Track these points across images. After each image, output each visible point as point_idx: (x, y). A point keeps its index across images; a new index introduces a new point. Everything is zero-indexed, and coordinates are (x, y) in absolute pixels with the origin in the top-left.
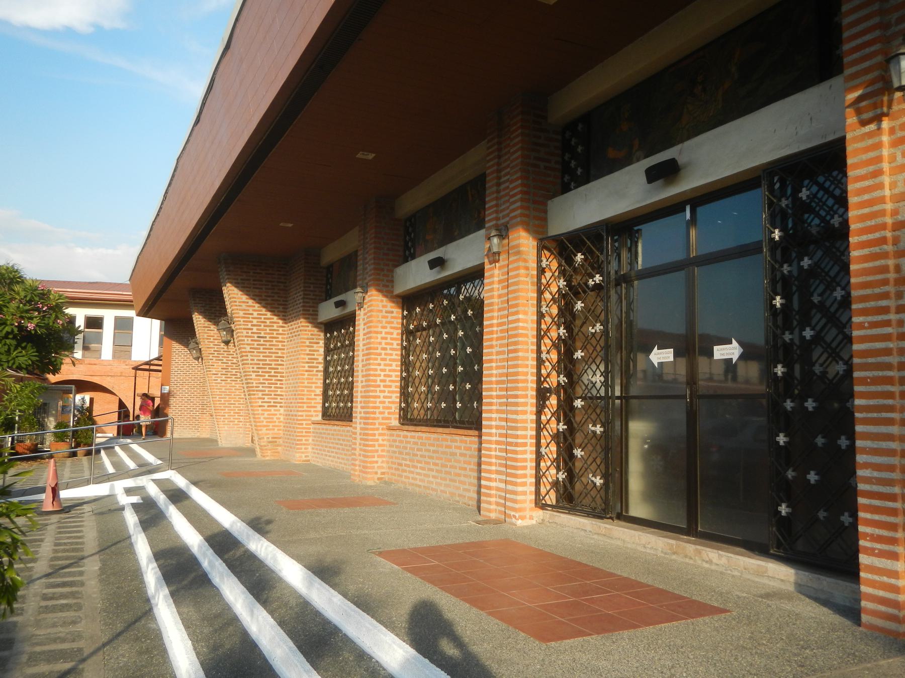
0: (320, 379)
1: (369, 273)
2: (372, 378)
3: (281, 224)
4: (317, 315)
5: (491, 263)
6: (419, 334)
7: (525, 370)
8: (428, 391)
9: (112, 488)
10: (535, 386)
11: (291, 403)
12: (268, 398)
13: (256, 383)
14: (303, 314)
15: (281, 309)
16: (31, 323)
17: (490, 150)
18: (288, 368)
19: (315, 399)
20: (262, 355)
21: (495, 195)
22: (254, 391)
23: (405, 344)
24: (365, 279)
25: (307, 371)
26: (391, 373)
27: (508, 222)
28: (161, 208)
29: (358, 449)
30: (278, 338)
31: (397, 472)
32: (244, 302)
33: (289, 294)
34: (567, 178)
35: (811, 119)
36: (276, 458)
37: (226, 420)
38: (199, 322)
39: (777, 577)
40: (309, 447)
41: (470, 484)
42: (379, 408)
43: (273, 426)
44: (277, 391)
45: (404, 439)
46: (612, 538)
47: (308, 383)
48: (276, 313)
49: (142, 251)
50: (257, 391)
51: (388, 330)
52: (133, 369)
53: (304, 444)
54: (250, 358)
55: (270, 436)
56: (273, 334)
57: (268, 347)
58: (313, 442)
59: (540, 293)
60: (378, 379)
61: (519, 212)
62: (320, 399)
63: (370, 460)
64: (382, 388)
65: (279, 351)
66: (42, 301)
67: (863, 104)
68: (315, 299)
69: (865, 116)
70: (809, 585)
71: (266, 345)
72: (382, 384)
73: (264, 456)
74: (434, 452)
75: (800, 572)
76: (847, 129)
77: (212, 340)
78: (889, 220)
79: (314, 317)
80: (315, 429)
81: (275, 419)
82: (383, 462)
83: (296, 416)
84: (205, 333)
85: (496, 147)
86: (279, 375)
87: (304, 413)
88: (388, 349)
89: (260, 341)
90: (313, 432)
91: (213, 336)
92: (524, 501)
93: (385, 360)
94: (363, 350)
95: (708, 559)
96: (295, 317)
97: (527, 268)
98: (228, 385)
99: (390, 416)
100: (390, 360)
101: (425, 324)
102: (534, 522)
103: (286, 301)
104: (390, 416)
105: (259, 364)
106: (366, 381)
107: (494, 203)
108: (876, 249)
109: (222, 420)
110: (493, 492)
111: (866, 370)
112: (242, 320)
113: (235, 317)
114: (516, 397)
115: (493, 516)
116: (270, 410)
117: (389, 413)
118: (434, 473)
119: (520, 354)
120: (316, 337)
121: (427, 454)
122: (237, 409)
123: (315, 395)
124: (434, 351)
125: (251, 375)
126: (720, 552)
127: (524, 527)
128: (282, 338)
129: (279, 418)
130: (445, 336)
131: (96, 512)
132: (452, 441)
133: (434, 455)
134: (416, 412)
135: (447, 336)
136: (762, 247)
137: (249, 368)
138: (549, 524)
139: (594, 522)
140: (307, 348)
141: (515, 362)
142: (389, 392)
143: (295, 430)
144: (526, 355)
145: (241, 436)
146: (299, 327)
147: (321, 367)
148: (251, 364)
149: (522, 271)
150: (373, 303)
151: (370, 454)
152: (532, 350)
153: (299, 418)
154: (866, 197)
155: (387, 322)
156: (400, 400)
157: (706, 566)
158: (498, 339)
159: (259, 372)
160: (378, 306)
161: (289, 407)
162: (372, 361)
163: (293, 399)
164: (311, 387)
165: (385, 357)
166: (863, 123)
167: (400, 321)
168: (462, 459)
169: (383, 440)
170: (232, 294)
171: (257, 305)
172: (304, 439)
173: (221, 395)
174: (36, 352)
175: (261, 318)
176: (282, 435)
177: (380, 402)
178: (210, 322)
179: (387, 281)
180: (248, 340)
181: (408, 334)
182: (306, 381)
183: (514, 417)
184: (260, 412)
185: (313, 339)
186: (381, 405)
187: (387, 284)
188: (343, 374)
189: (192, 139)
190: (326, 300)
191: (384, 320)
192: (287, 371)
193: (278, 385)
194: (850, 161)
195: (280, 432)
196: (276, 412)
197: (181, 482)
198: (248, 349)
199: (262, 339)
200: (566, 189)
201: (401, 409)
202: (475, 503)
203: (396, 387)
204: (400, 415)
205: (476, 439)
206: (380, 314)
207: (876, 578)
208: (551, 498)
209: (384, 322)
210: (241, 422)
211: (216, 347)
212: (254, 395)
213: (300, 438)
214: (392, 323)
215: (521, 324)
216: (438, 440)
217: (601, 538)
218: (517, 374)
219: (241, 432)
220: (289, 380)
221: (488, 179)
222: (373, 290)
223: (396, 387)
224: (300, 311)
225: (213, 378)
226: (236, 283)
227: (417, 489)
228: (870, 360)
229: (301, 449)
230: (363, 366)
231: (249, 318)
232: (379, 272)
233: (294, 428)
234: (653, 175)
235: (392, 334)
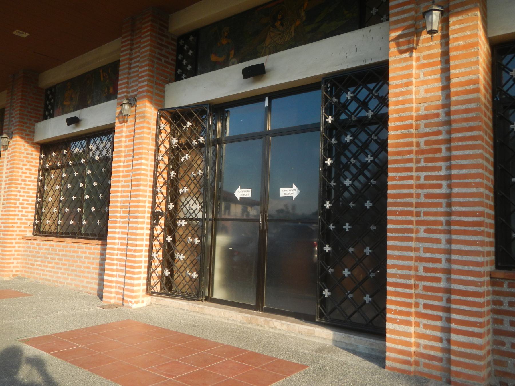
1: (15, 125)
2: (12, 201)
5: (120, 123)
6: (53, 171)
7: (144, 199)
8: (59, 213)
10: (150, 210)
17: (124, 44)
21: (127, 76)
23: (41, 178)
24: (11, 128)
26: (28, 198)
27: (136, 95)
31: (30, 270)
34: (179, 71)
35: (356, 49)
39: (321, 336)
41: (92, 278)
42: (17, 223)
45: (37, 246)
46: (203, 314)
51: (28, 167)
59: (158, 146)
60: (18, 202)
61: (146, 88)
63: (7, 261)
64: (20, 209)
67: (401, 40)
69: (403, 48)
70: (342, 341)
72: (20, 206)
74: (63, 255)
75: (336, 333)
76: (390, 55)
78: (414, 114)
85: (129, 42)
88: (27, 181)
92: (138, 291)
93: (24, 188)
94: (5, 181)
95: (273, 327)
97: (149, 129)
99: (25, 229)
101: (59, 164)
102: (144, 305)
104: (25, 229)
106: (7, 203)
107: (126, 81)
108: (406, 131)
110: (114, 284)
111: (396, 207)
114: (137, 217)
115: (113, 301)
117: (25, 227)
118: (62, 271)
119: (142, 188)
121: (57, 257)
124: (66, 184)
126: (283, 322)
127: (137, 309)
130: (76, 173)
132: (78, 248)
133: (63, 258)
134: (47, 227)
135: (77, 174)
136: (320, 127)
138: (155, 306)
139: (190, 304)
141: (137, 193)
142: (26, 212)
144: (145, 188)
149: (146, 130)
150: (17, 146)
151: (7, 257)
152: (150, 186)
154: (401, 98)
155: (27, 161)
156: (35, 218)
157: (272, 331)
158: (123, 176)
160: (20, 149)
162: (13, 189)
165: (24, 186)
166: (401, 52)
167: (38, 161)
168: (86, 260)
169: (19, 247)
177: (18, 219)
179: (30, 131)
181: (44, 171)
183: (134, 231)
191: (25, 160)
194: (391, 75)
200: (178, 78)
201: (35, 224)
202: (96, 292)
203: (32, 209)
204: (34, 229)
205: (99, 247)
206: (22, 155)
207: (397, 337)
208: (158, 288)
214: (32, 162)
215: (143, 167)
216: (67, 247)
217: (195, 314)
218: (138, 201)
221: (121, 64)
227: (47, 283)
228: (399, 200)
230: (5, 192)
232: (22, 124)
234: (248, 73)
235: (31, 170)
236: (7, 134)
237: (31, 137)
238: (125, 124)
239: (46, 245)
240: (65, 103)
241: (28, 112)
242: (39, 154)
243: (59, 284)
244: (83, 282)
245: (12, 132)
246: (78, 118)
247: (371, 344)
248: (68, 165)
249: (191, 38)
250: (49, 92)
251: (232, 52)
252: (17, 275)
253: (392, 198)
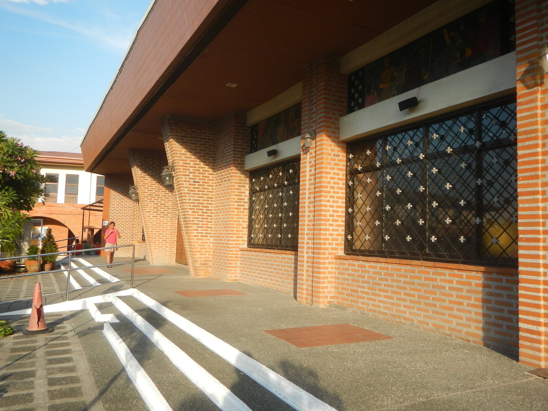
0: (245, 215)
1: (318, 121)
3: (228, 85)
4: (244, 164)
5: (528, 87)
9: (85, 304)
11: (222, 234)
12: (201, 230)
13: (192, 218)
14: (234, 163)
15: (211, 160)
16: (13, 171)
18: (217, 207)
19: (243, 231)
20: (196, 196)
22: (190, 224)
24: (312, 127)
25: (236, 209)
26: (338, 209)
28: (115, 81)
29: (305, 275)
30: (209, 183)
32: (183, 154)
33: (217, 149)
36: (207, 277)
37: (157, 246)
38: (137, 174)
40: (238, 269)
42: (328, 239)
43: (205, 252)
44: (208, 224)
47: (237, 218)
48: (207, 163)
49: (94, 121)
50: (193, 224)
51: (336, 171)
52: (82, 209)
53: (234, 267)
54: (187, 198)
55: (203, 259)
56: (205, 179)
57: (201, 190)
58: (241, 266)
60: (328, 214)
62: (246, 231)
64: (331, 222)
65: (210, 193)
66: (20, 155)
68: (242, 152)
71: (199, 188)
72: (331, 218)
73: (198, 275)
77: (146, 187)
79: (242, 166)
80: (243, 255)
81: (206, 246)
82: (331, 287)
83: (227, 244)
84: (142, 181)
86: (209, 212)
87: (234, 242)
88: (336, 188)
89: (195, 185)
90: (241, 258)
91: (148, 184)
93: (332, 197)
94: (309, 189)
96: (224, 166)
98: (158, 220)
99: (337, 247)
100: (337, 197)
103: (215, 154)
104: (337, 247)
105: (194, 203)
109: (154, 245)
112: (182, 168)
113: (176, 166)
116: (203, 239)
117: (336, 244)
120: (244, 182)
122: (164, 238)
123: (242, 228)
125: (189, 212)
128: (212, 183)
129: (210, 246)
131: (77, 331)
137: (187, 206)
140: (236, 190)
143: (226, 255)
145: (168, 257)
146: (230, 173)
147: (247, 206)
148: (189, 203)
153: (230, 246)
155: (335, 164)
159: (194, 209)
161: (219, 237)
163: (223, 231)
164: (239, 221)
165: (333, 195)
167: (345, 163)
169: (332, 268)
170: (174, 147)
171: (193, 157)
172: (234, 262)
173: (153, 227)
174: (16, 193)
175: (196, 167)
176: (211, 259)
177: (330, 235)
178: (146, 173)
179: (335, 128)
180: (186, 184)
181: (352, 174)
182: (235, 217)
184: (195, 241)
185: (241, 183)
186: (330, 237)
187: (335, 130)
188: (270, 211)
189: (156, 7)
190: (251, 152)
191: (333, 162)
192: (216, 208)
193: (209, 220)
195: (211, 256)
196: (207, 241)
197: (150, 302)
198: (186, 191)
199: (197, 184)
203: (342, 221)
205: (480, 275)
206: (329, 157)
209: (332, 164)
210: (168, 247)
211: (149, 192)
212: (191, 227)
213: (231, 262)
214: (339, 165)
219: (167, 254)
220: (219, 216)
222: (324, 135)
224: (231, 161)
225: (147, 215)
226: (177, 139)
229: (232, 270)
231: (187, 167)
232: (328, 120)
233: (224, 253)
235: (338, 174)
236: (309, 134)
237: (336, 135)
238: (539, 88)
242: (345, 154)
243: (403, 321)
245: (315, 131)
248: (394, 164)
252: (331, 302)
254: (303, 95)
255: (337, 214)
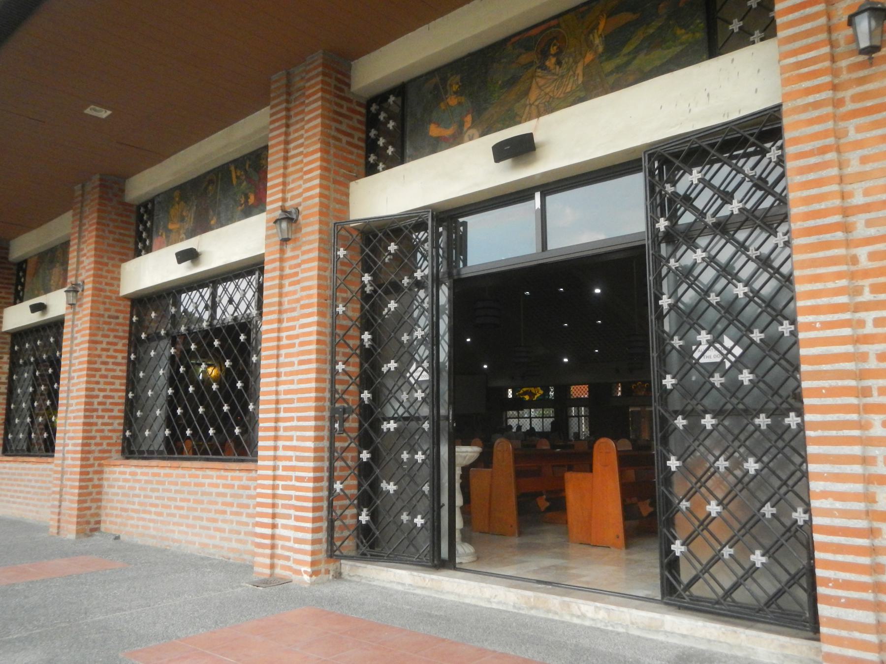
17: (274, 118)
27: (299, 204)
34: (372, 158)
35: (708, 95)
46: (441, 592)
51: (111, 339)
64: (100, 413)
70: (721, 640)
72: (100, 407)
74: (176, 492)
88: (110, 364)
93: (106, 377)
95: (579, 614)
100: (113, 377)
111: (819, 380)
117: (108, 444)
132: (204, 477)
142: (110, 417)
154: (812, 176)
155: (109, 330)
157: (576, 621)
177: (97, 431)
186: (98, 435)
190: (15, 303)
191: (106, 327)
200: (371, 170)
203: (118, 411)
207: (844, 633)
214: (117, 331)
221: (270, 151)
223: (119, 411)
228: (824, 367)
232: (100, 266)
234: (501, 152)
239: (146, 474)
240: (171, 226)
241: (109, 245)
244: (214, 537)
246: (195, 250)
247: (783, 646)
249: (392, 99)
250: (142, 210)
251: (469, 119)
253: (810, 364)
254: (73, 228)
255: (111, 401)
